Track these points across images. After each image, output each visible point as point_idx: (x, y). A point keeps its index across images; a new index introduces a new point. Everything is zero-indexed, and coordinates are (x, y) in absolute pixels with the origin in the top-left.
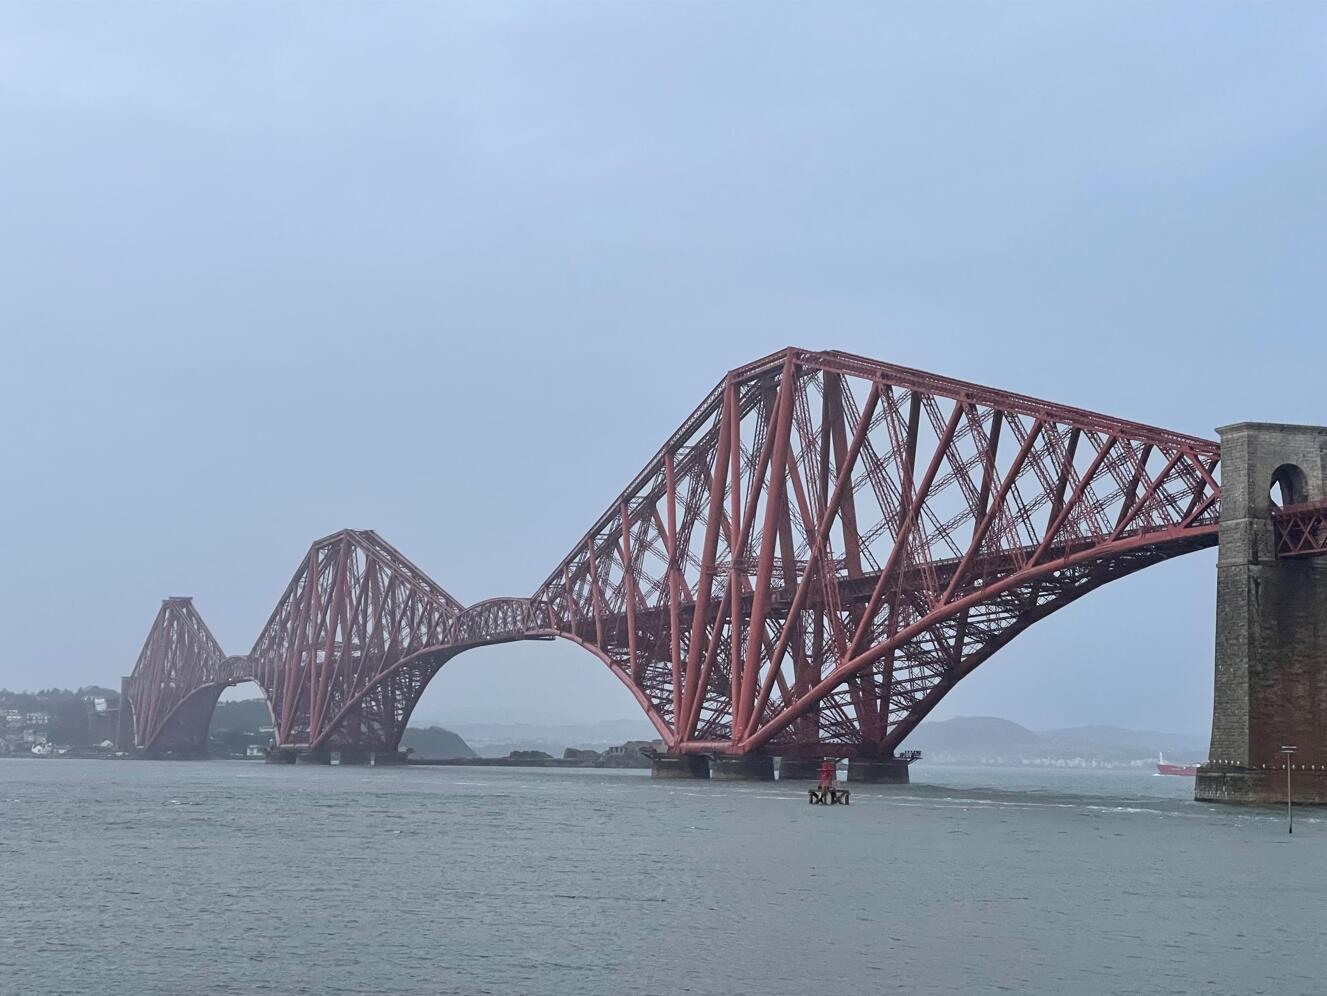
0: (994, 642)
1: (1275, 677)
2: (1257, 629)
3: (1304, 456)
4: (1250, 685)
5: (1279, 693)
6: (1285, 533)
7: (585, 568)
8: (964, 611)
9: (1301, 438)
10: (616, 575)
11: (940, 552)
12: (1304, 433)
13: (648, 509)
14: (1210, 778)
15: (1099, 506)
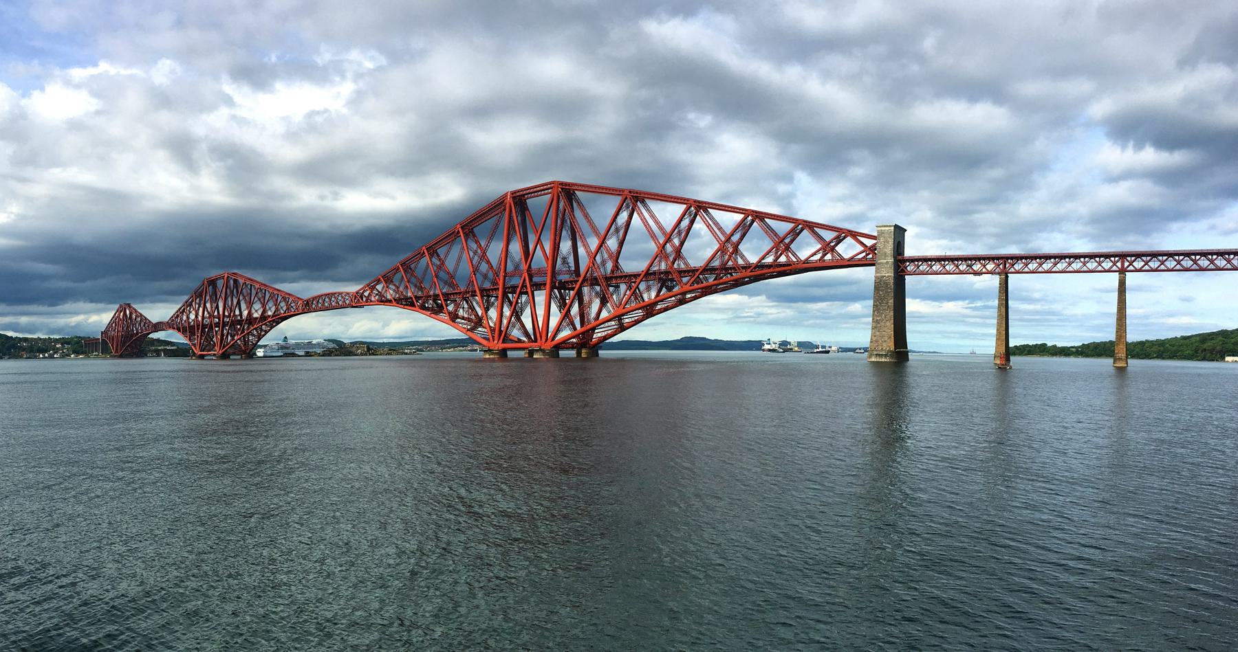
0: (266, 332)
7: (178, 316)
8: (261, 326)
10: (185, 318)
11: (256, 315)
13: (191, 305)
15: (282, 308)
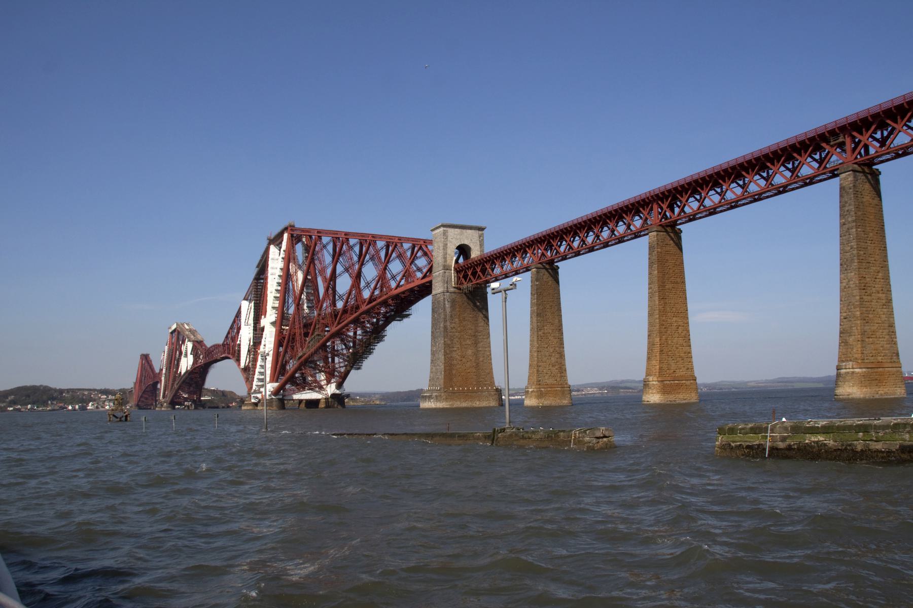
1: (457, 346)
2: (448, 324)
3: (471, 240)
4: (445, 351)
5: (459, 354)
6: (461, 277)
9: (469, 231)
12: (471, 229)
14: (426, 396)
